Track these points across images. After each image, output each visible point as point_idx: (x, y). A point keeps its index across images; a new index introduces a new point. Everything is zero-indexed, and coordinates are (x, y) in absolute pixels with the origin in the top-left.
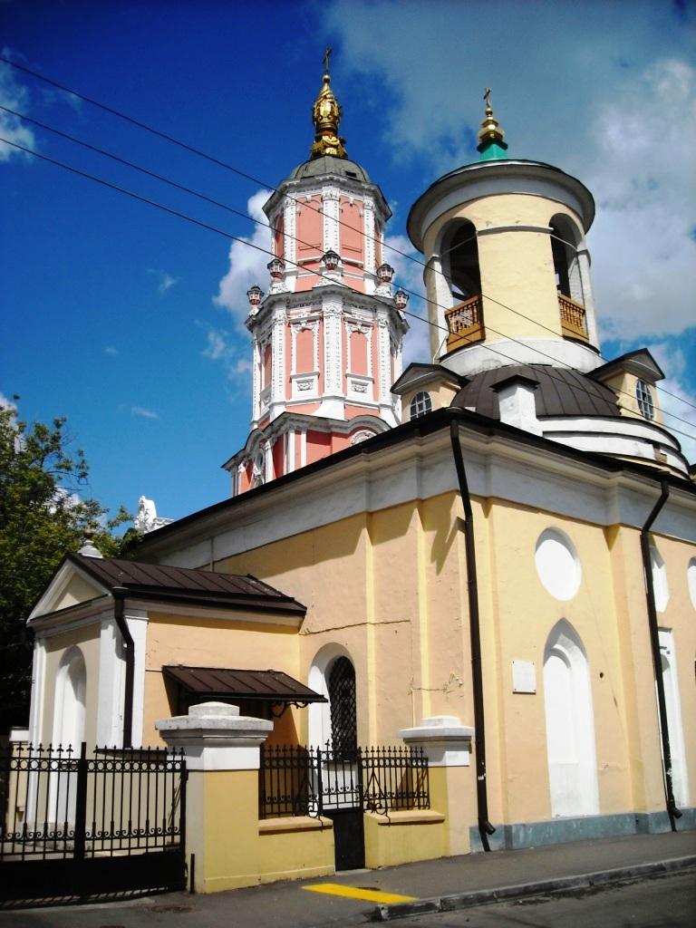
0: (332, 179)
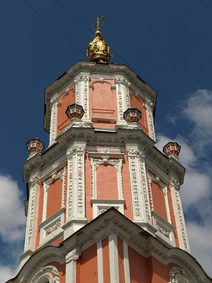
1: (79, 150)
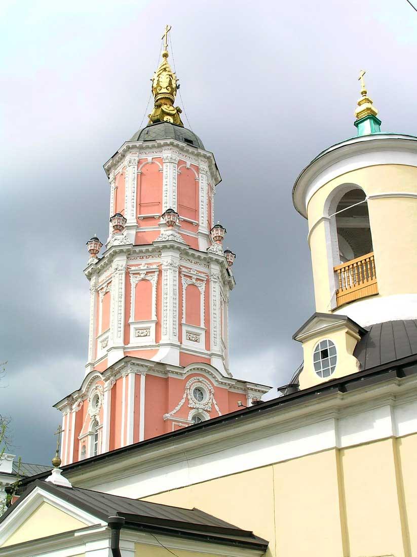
0: (172, 144)
1: (120, 268)
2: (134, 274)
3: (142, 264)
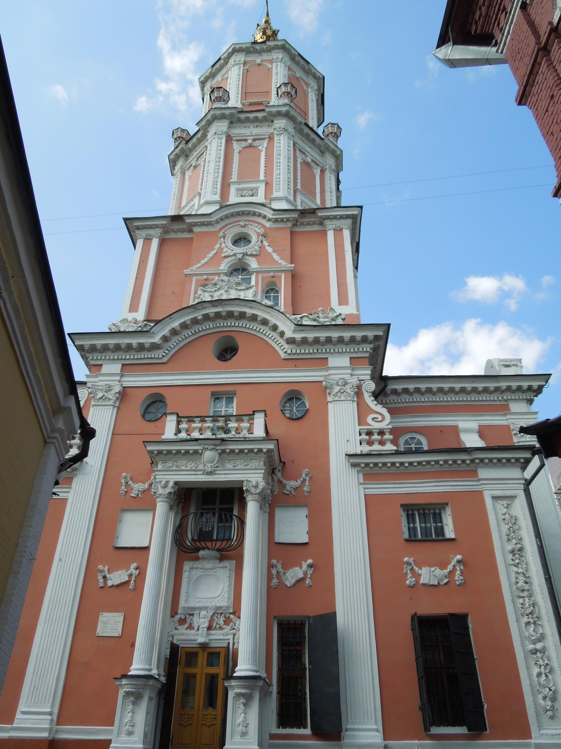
2: (237, 140)
3: (250, 131)
